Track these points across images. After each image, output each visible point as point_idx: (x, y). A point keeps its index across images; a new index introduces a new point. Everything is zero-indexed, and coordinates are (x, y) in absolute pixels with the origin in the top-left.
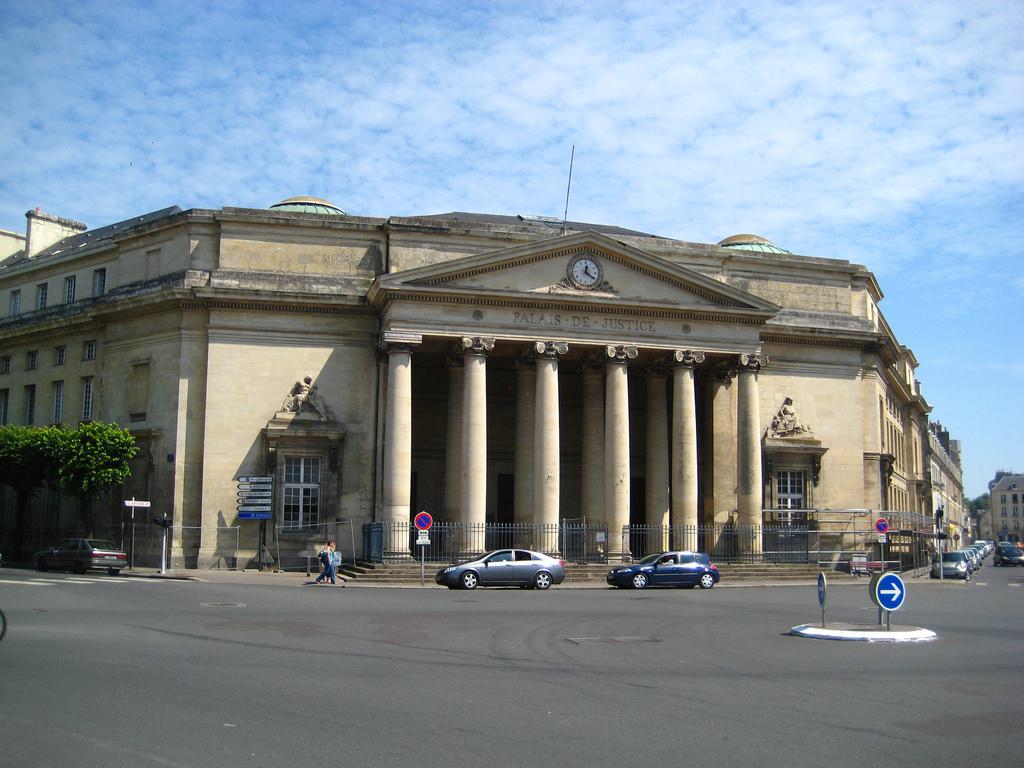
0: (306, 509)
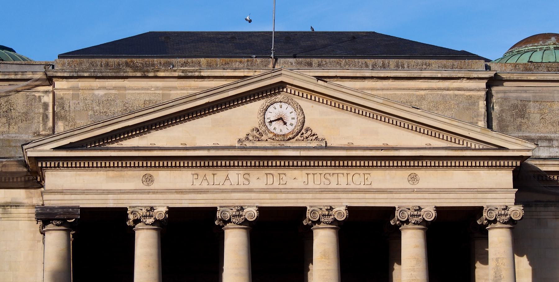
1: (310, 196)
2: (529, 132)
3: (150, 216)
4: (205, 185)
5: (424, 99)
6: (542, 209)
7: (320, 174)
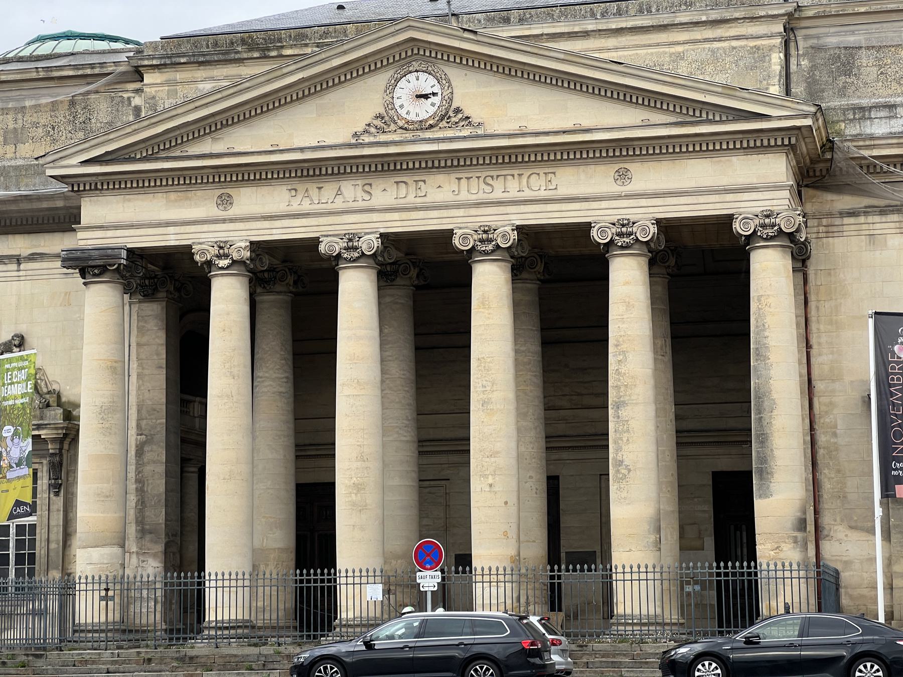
0: (19, 559)
1: (461, 212)
2: (859, 97)
3: (226, 256)
4: (306, 206)
5: (682, 59)
6: (877, 219)
7: (478, 177)
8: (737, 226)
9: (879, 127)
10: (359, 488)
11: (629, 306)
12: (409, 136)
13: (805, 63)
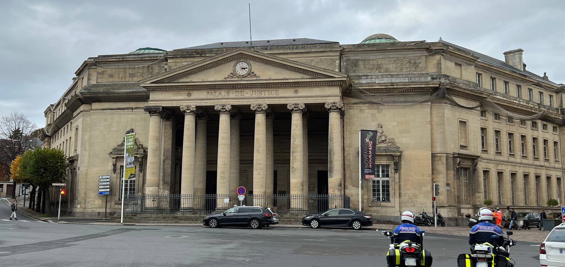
1: (253, 100)
3: (189, 109)
4: (211, 97)
8: (326, 106)
9: (364, 81)
10: (223, 172)
11: (297, 126)
12: (240, 79)
13: (345, 63)
